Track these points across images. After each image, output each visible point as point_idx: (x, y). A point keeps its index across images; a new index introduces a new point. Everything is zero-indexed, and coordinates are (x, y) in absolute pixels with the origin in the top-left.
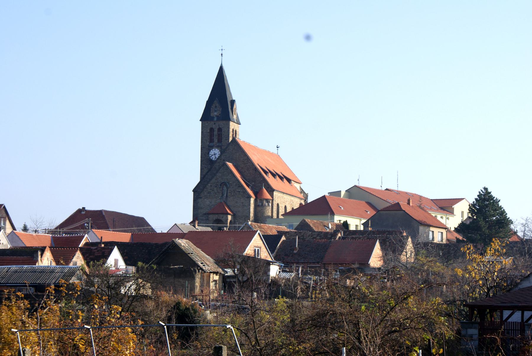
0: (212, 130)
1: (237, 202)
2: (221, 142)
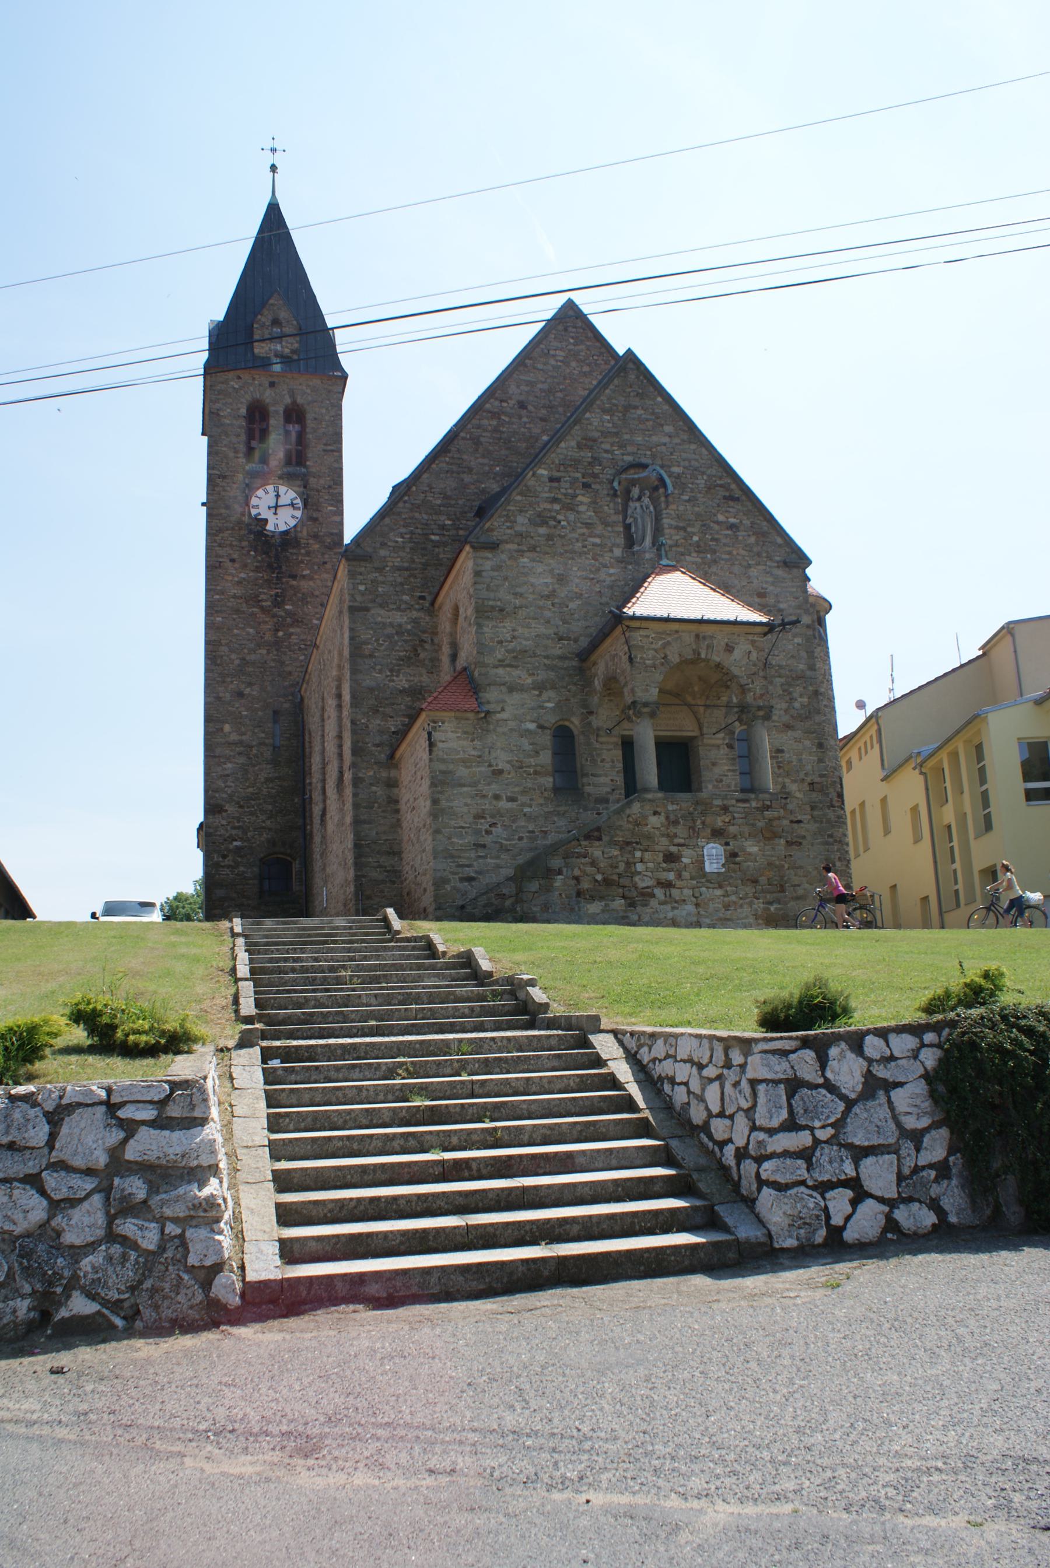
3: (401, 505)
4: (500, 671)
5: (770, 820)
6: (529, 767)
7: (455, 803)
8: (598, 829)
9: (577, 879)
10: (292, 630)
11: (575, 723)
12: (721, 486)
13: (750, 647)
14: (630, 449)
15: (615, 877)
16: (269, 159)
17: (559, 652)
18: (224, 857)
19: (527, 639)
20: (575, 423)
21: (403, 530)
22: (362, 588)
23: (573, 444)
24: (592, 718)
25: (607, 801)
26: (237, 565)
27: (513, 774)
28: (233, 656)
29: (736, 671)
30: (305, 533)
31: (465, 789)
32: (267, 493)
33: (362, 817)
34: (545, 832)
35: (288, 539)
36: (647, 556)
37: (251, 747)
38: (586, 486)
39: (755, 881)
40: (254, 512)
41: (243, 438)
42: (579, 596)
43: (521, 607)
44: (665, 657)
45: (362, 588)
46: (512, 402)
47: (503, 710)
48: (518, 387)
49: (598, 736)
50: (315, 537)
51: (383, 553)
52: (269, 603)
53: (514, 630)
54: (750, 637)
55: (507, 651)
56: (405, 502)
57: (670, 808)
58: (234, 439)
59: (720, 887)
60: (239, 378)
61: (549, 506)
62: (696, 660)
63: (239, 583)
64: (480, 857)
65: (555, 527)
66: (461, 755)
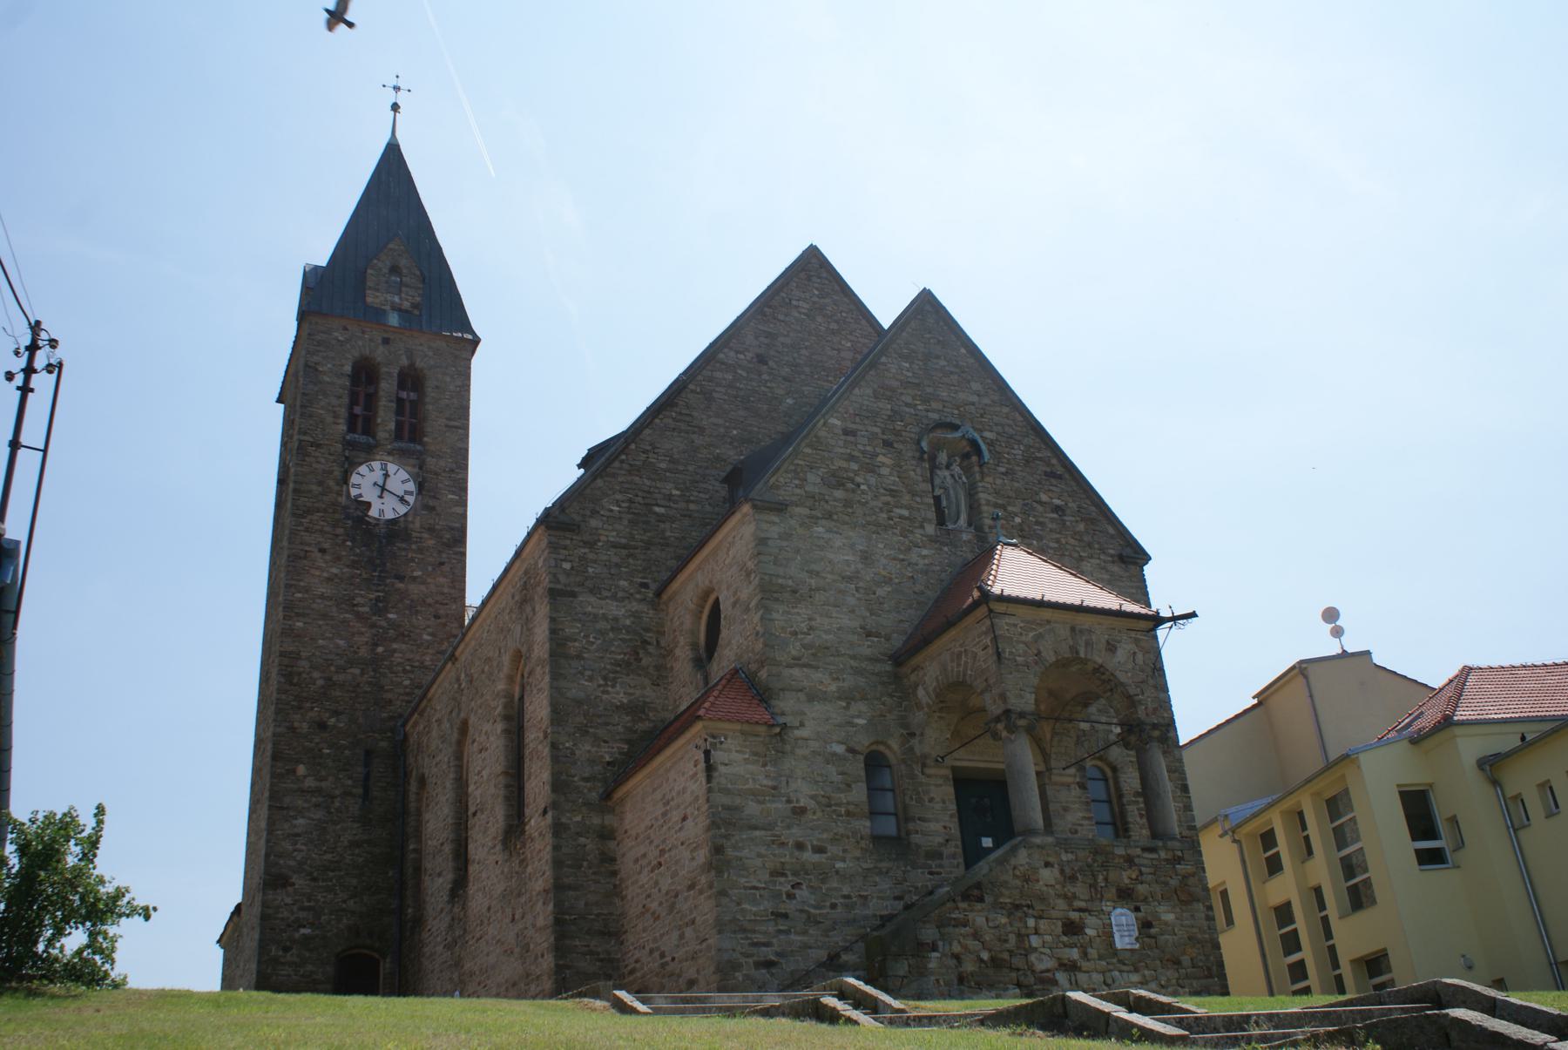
0: (365, 374)
3: (616, 464)
4: (796, 672)
5: (1184, 877)
6: (839, 805)
7: (745, 852)
8: (979, 886)
9: (957, 957)
10: (395, 646)
11: (894, 748)
12: (1040, 459)
13: (1132, 647)
14: (934, 405)
15: (1006, 956)
16: (391, 97)
17: (868, 652)
18: (286, 950)
19: (827, 632)
20: (873, 365)
21: (618, 496)
22: (567, 566)
23: (869, 391)
24: (915, 741)
25: (940, 856)
26: (328, 557)
27: (819, 814)
28: (316, 675)
29: (1122, 677)
30: (417, 525)
31: (757, 833)
32: (372, 470)
33: (566, 880)
34: (865, 898)
35: (395, 530)
36: (965, 537)
37: (333, 797)
38: (887, 444)
39: (1177, 963)
40: (354, 492)
41: (346, 400)
42: (888, 581)
43: (818, 589)
44: (1038, 654)
45: (567, 566)
46: (749, 355)
47: (802, 725)
48: (756, 338)
49: (924, 765)
50: (431, 530)
51: (594, 523)
52: (366, 609)
53: (810, 619)
54: (1133, 634)
55: (804, 646)
56: (622, 462)
57: (1064, 857)
58: (334, 401)
59: (1136, 970)
60: (345, 329)
61: (844, 464)
62: (1076, 659)
63: (329, 579)
64: (780, 931)
65: (853, 491)
66: (750, 785)
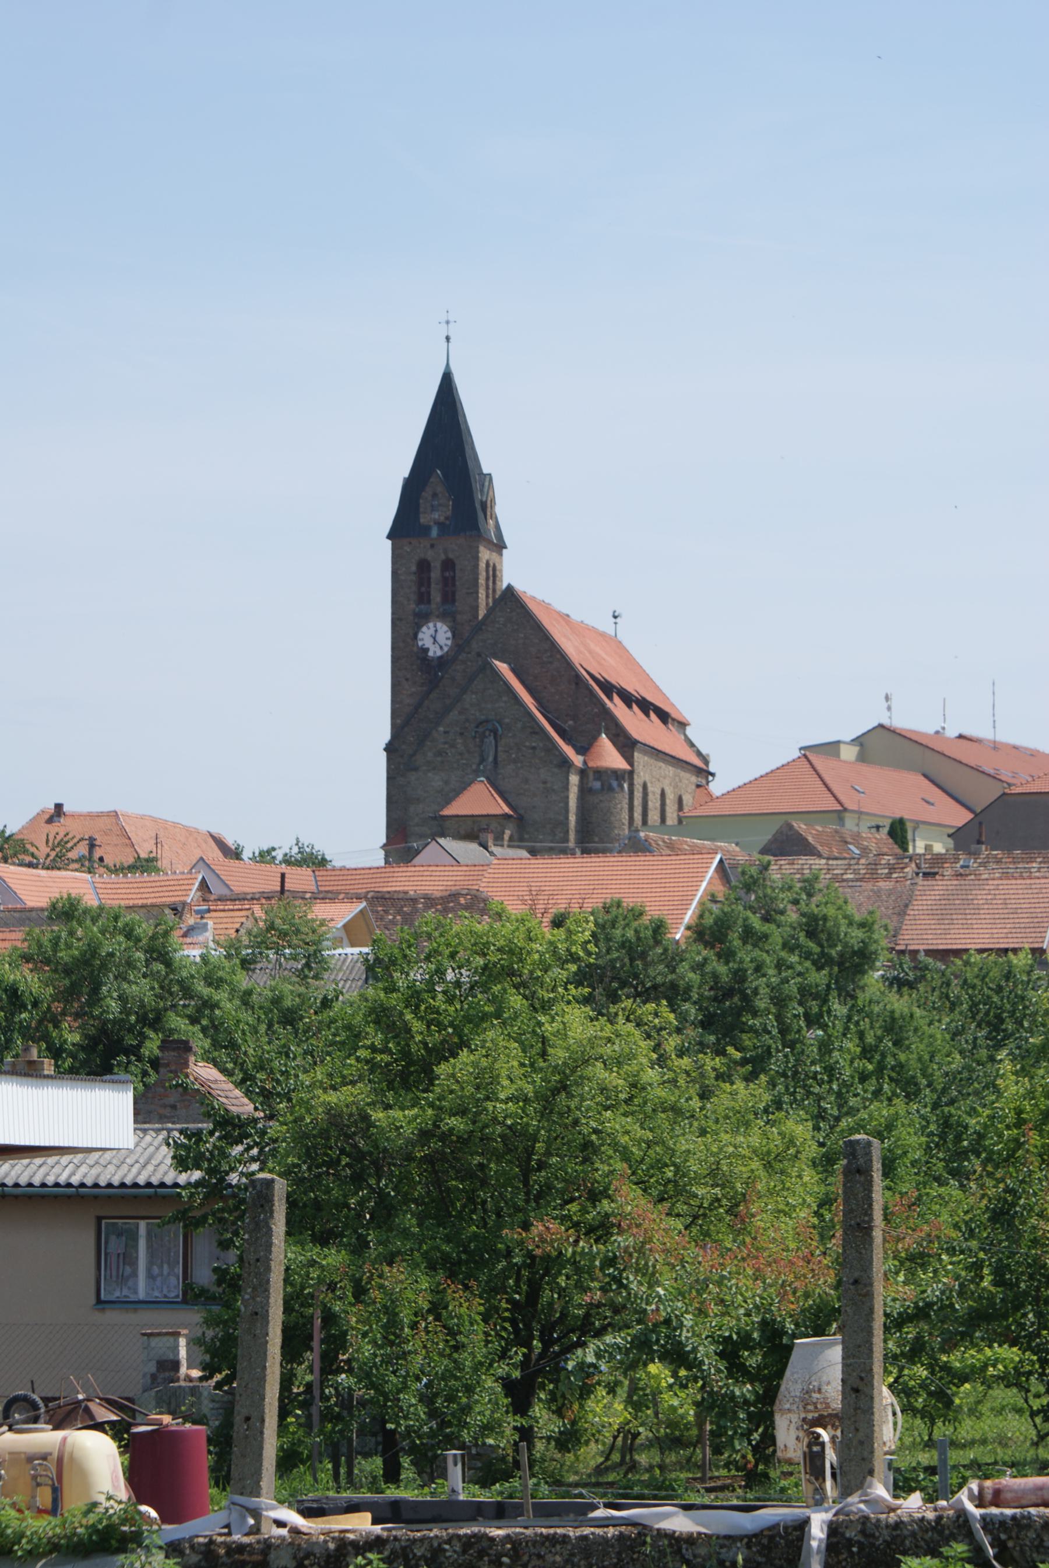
0: (424, 566)
1: (526, 781)
2: (454, 601)
4: (416, 828)
38: (462, 734)
40: (420, 643)
51: (404, 747)
